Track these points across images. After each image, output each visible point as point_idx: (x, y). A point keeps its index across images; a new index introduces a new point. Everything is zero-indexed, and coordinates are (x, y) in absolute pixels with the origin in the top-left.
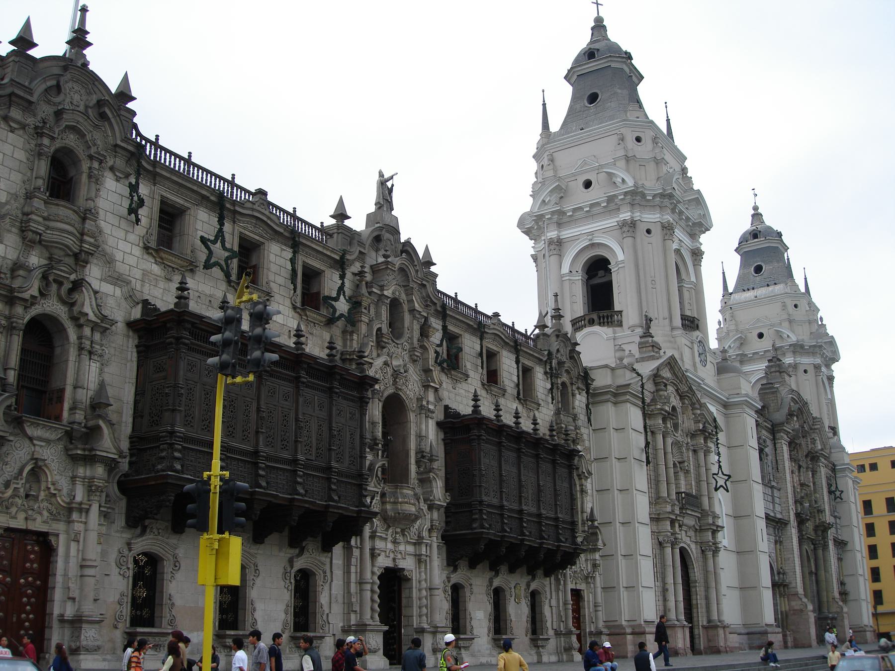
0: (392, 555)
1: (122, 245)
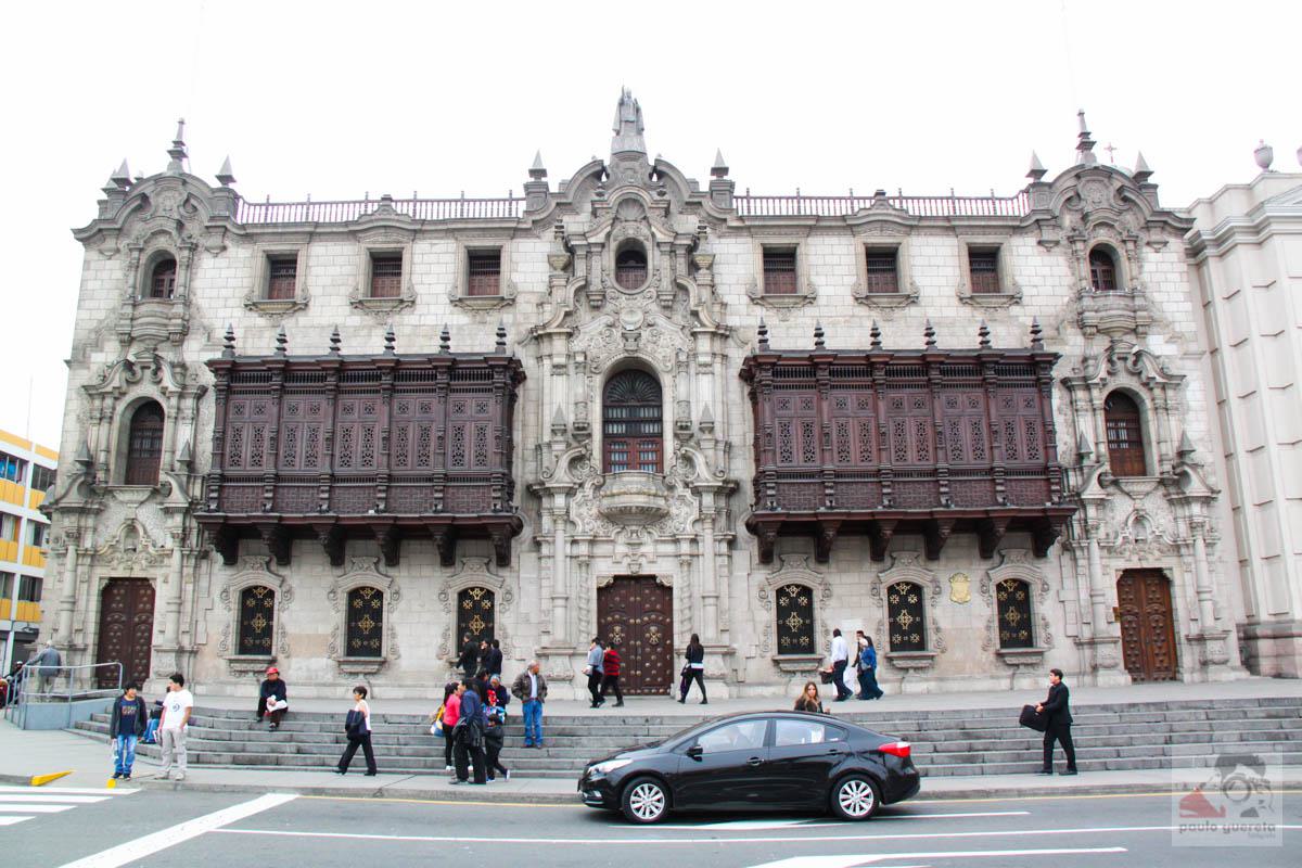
0: (627, 561)
1: (222, 313)
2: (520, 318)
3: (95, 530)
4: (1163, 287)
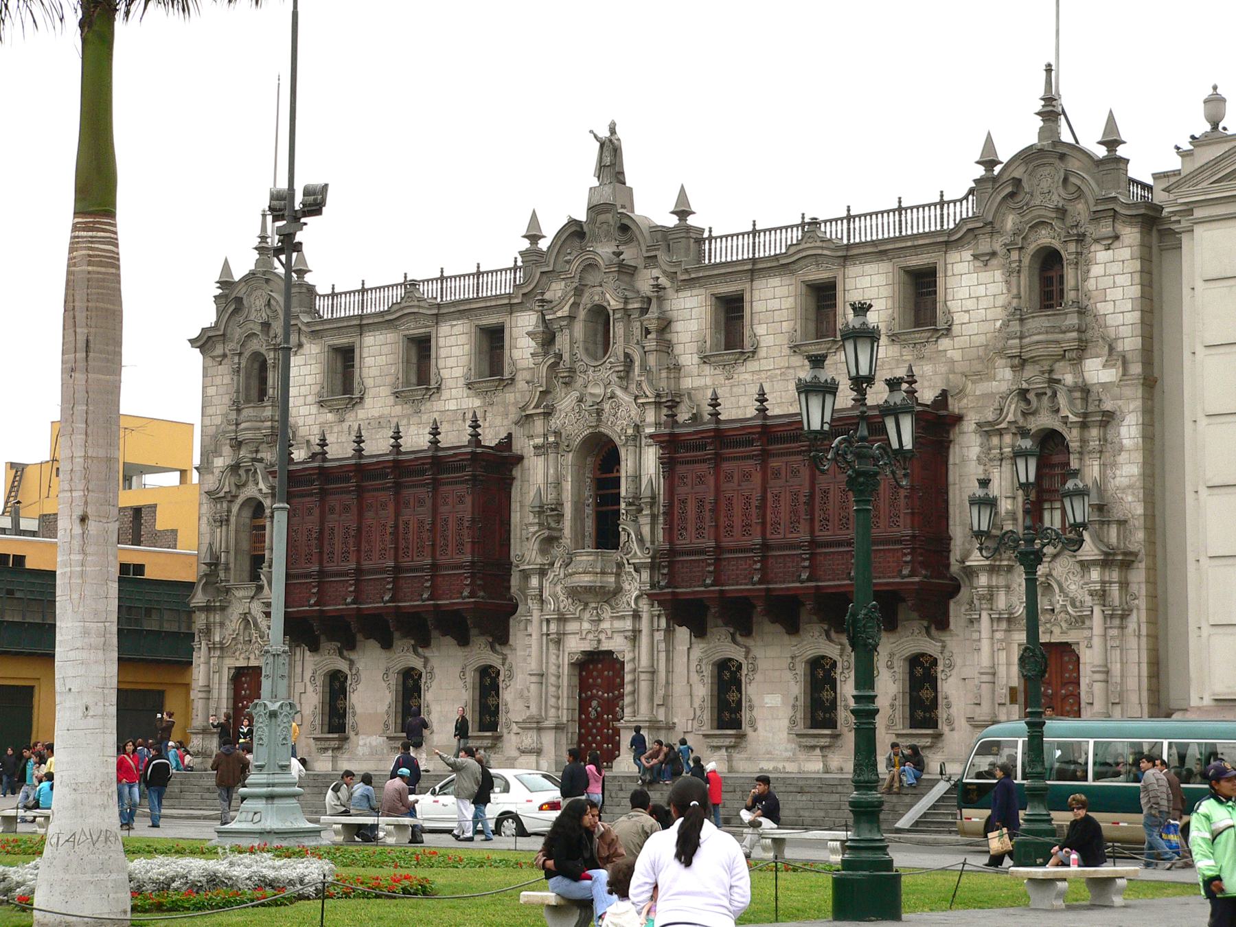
3: (222, 624)
4: (1111, 295)
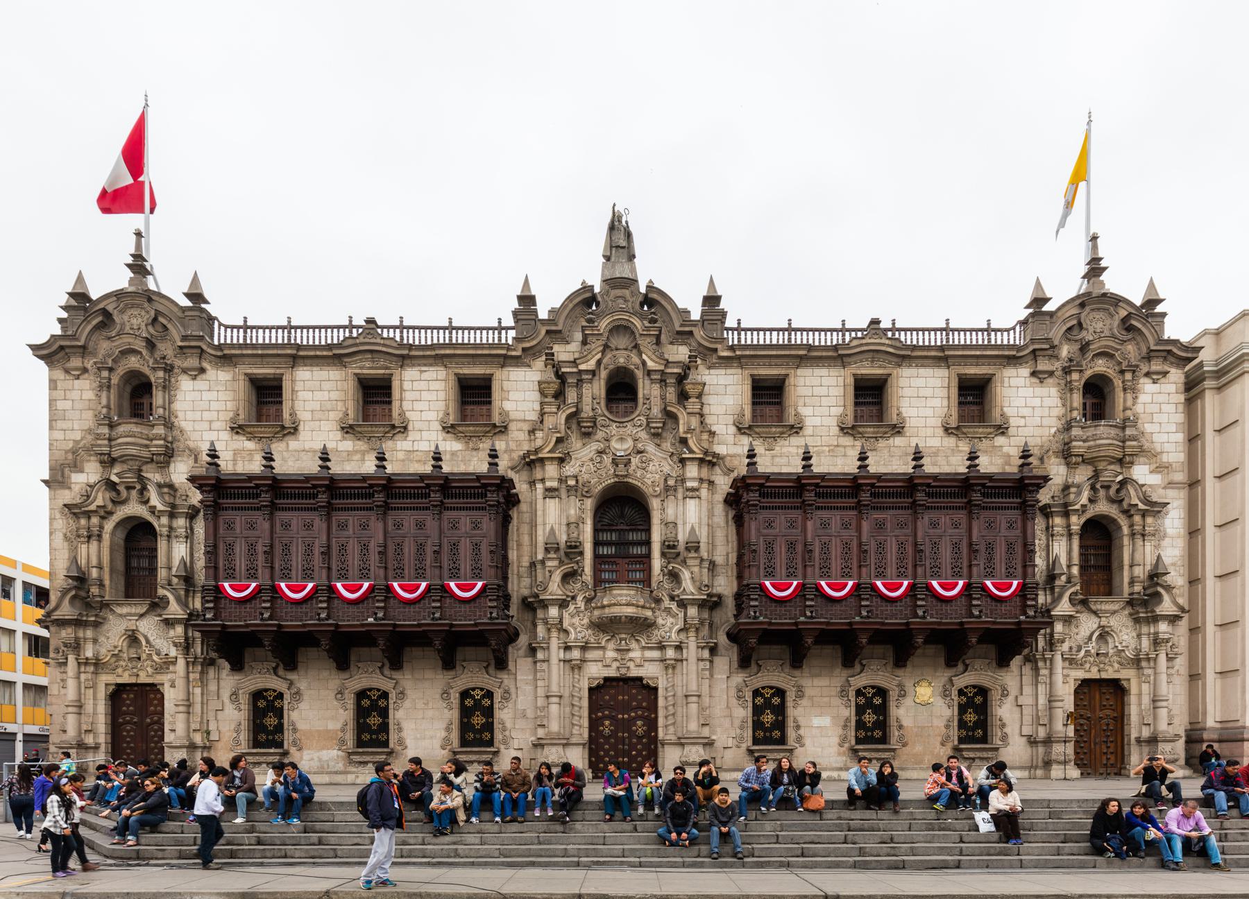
2: (513, 445)
